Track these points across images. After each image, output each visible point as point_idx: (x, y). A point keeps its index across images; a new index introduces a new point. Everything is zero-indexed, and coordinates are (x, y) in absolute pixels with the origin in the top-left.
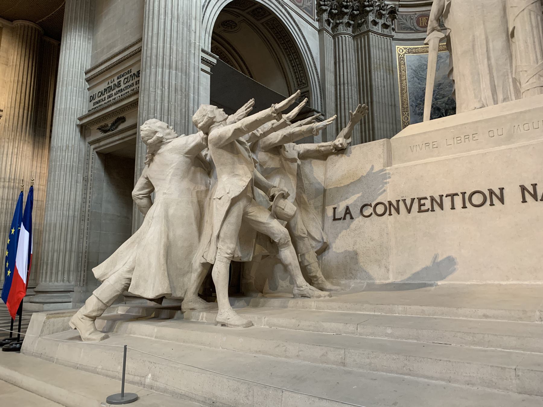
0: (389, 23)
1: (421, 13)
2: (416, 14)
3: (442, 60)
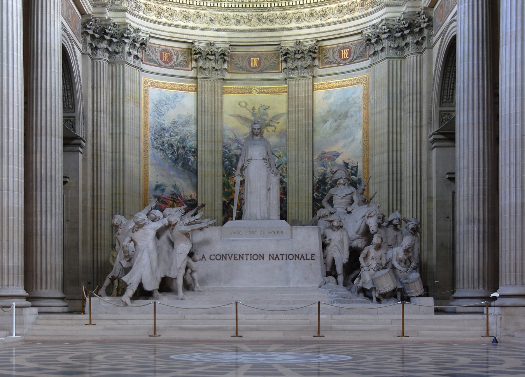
0: (140, 55)
1: (164, 47)
2: (160, 47)
3: (178, 100)
